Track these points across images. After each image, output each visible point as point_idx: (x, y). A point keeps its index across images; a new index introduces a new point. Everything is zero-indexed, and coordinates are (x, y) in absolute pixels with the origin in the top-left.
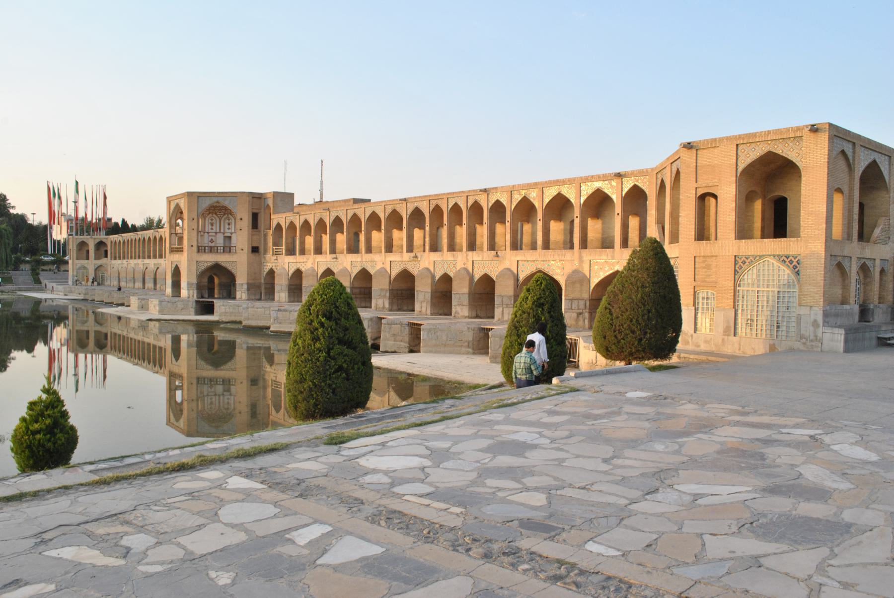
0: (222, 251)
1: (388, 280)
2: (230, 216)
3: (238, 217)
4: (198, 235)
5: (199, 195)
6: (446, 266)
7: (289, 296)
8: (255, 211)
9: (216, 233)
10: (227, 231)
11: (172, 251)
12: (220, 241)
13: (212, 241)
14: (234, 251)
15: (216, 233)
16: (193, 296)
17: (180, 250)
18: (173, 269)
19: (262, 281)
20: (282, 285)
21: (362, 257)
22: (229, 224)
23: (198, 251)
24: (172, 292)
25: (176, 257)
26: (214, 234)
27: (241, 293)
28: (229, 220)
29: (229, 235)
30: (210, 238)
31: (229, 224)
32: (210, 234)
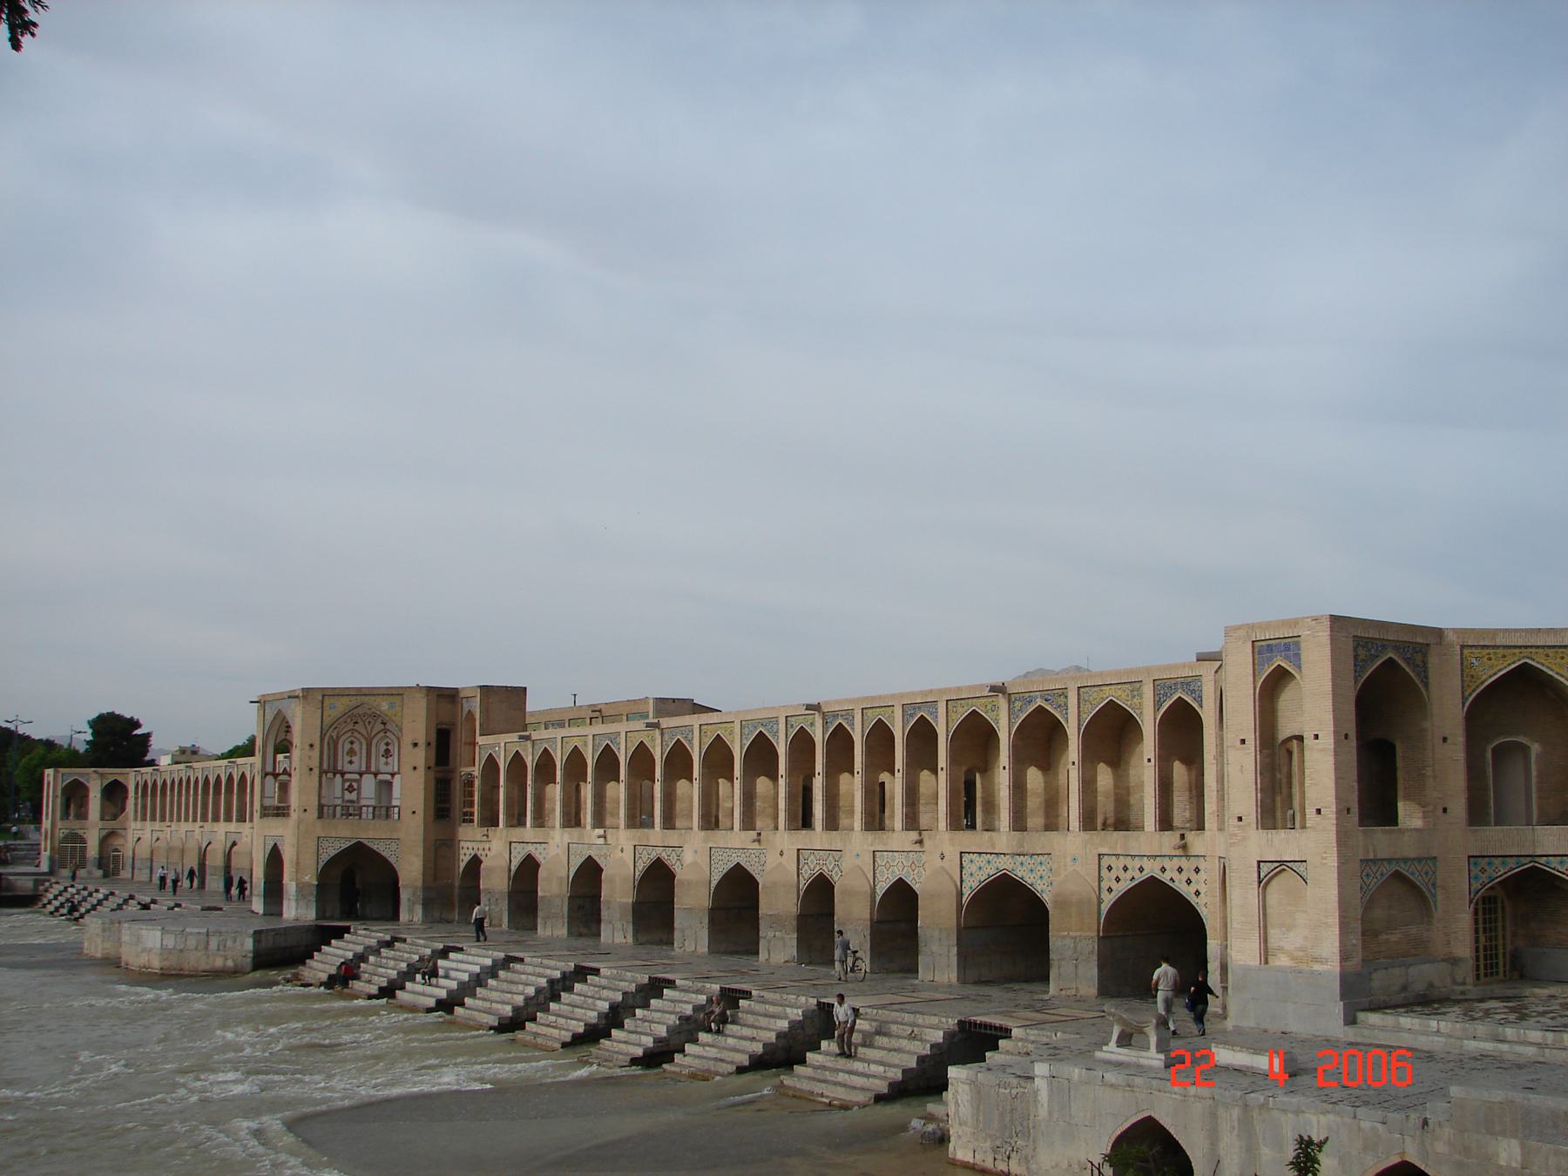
0: (371, 816)
4: (320, 777)
8: (444, 727)
10: (383, 768)
11: (266, 812)
13: (351, 789)
14: (396, 816)
15: (361, 774)
17: (281, 812)
18: (268, 851)
23: (321, 815)
26: (357, 777)
27: (411, 912)
28: (387, 744)
29: (388, 777)
30: (347, 784)
32: (347, 776)
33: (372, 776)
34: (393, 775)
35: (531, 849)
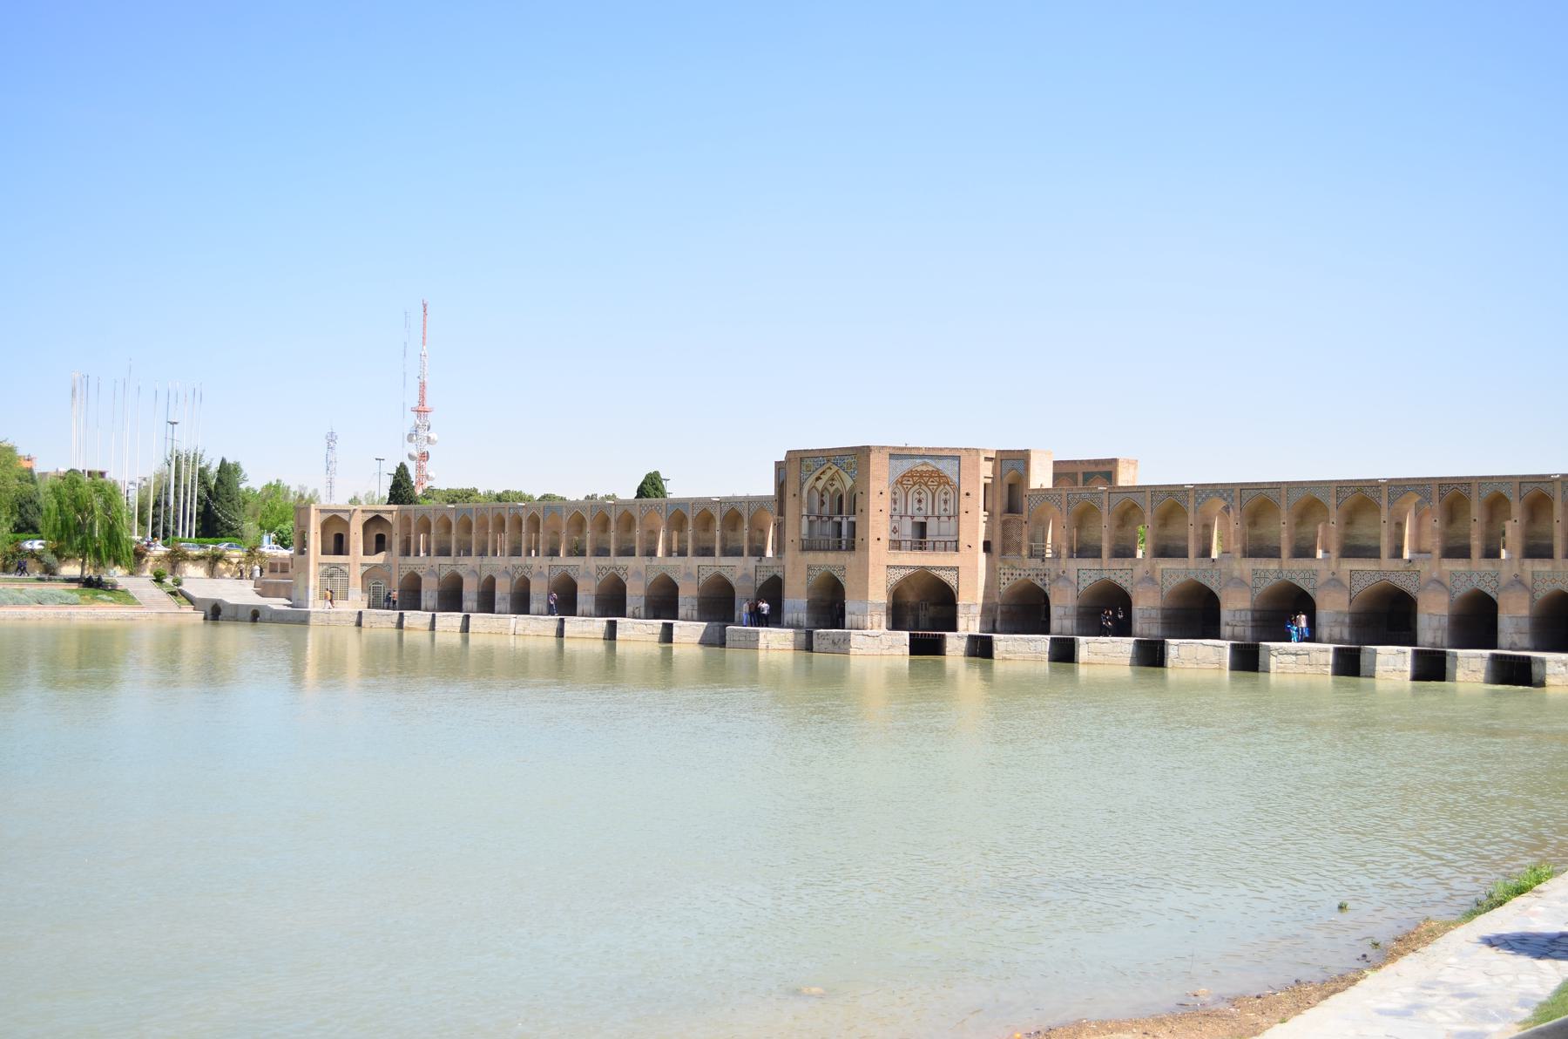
1: (1347, 598)
2: (923, 487)
3: (963, 492)
5: (892, 452)
6: (1476, 579)
7: (1078, 625)
9: (901, 517)
12: (907, 530)
15: (901, 517)
16: (880, 626)
19: (997, 600)
20: (1066, 607)
21: (1281, 566)
22: (920, 501)
24: (808, 619)
25: (828, 561)
26: (898, 518)
28: (919, 493)
29: (923, 520)
31: (920, 501)
33: (909, 518)
34: (927, 517)
35: (1105, 575)
